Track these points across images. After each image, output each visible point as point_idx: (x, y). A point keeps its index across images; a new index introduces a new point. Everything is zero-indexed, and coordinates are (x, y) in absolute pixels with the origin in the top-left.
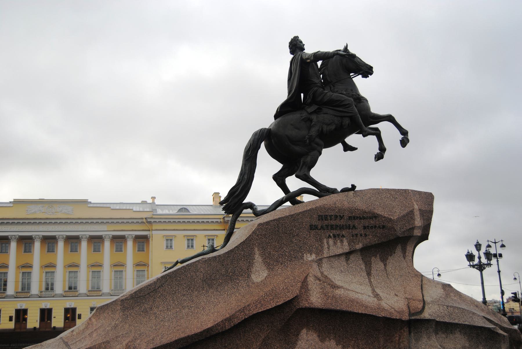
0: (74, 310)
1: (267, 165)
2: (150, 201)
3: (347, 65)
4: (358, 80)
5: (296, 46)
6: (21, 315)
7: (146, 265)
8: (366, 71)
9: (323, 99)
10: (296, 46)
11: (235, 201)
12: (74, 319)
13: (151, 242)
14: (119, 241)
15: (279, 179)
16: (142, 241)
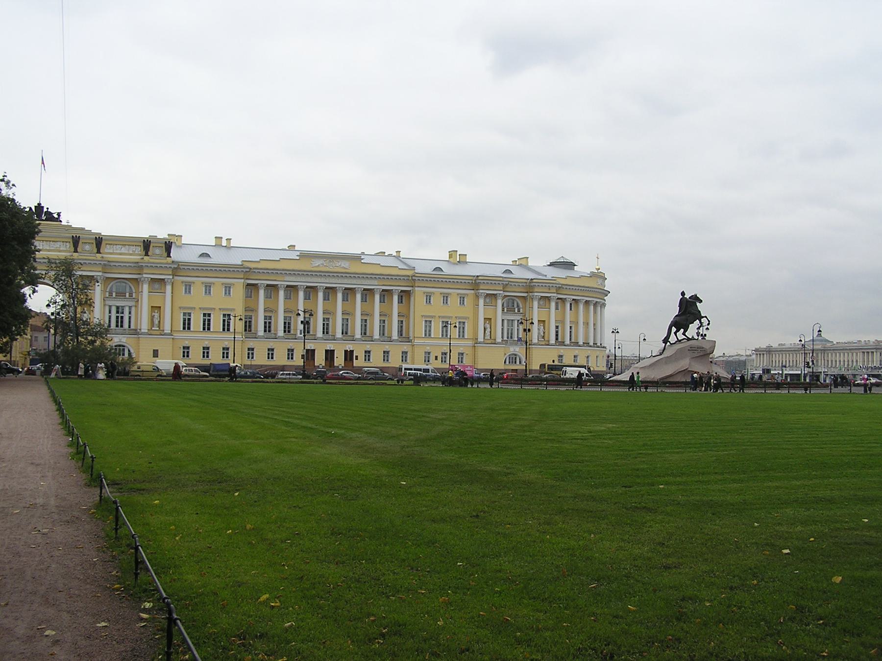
0: (352, 352)
1: (674, 329)
2: (395, 254)
3: (696, 299)
4: (698, 304)
5: (683, 294)
6: (310, 355)
7: (408, 317)
8: (701, 301)
9: (688, 310)
10: (683, 294)
11: (666, 340)
12: (352, 360)
13: (412, 299)
14: (386, 294)
15: (675, 333)
16: (405, 296)
